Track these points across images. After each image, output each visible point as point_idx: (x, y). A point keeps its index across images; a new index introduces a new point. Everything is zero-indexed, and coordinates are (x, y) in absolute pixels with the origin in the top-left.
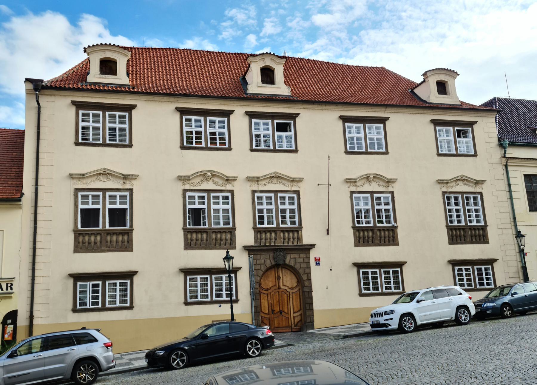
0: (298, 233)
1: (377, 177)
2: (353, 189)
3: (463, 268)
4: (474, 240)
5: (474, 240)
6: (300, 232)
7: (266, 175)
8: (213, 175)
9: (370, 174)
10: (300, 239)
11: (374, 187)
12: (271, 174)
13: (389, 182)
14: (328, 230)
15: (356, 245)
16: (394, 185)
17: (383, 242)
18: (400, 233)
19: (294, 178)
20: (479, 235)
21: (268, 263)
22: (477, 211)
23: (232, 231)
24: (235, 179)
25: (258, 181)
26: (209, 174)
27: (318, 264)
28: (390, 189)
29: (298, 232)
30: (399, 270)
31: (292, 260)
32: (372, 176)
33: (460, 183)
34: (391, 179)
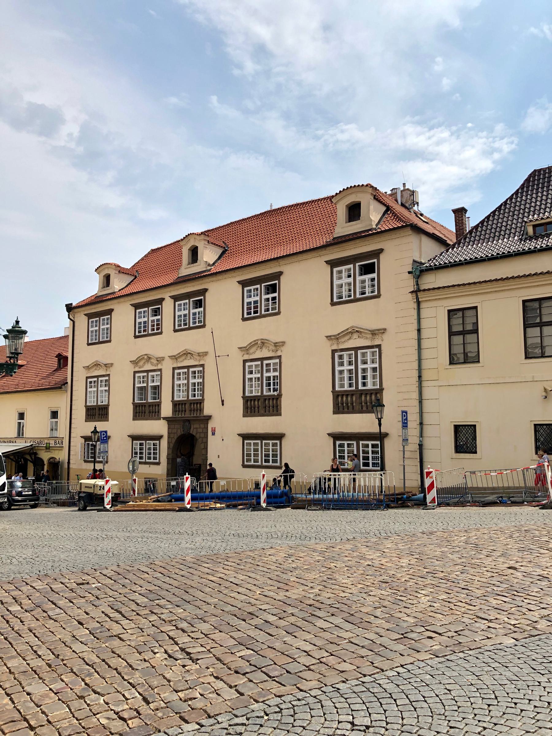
0: (200, 405)
1: (263, 343)
2: (246, 357)
3: (346, 443)
4: (364, 409)
5: (364, 409)
6: (202, 404)
7: (179, 353)
8: (150, 358)
9: (257, 340)
10: (201, 410)
11: (265, 353)
12: (183, 351)
13: (278, 345)
14: (223, 401)
15: (244, 416)
16: (282, 348)
17: (267, 412)
18: (285, 403)
19: (198, 353)
20: (371, 401)
21: (180, 432)
22: (374, 369)
23: (159, 405)
24: (163, 359)
25: (176, 359)
26: (146, 357)
27: (213, 434)
28: (279, 353)
29: (201, 403)
30: (278, 442)
31: (195, 430)
32: (259, 342)
33: (355, 335)
34: (276, 343)
